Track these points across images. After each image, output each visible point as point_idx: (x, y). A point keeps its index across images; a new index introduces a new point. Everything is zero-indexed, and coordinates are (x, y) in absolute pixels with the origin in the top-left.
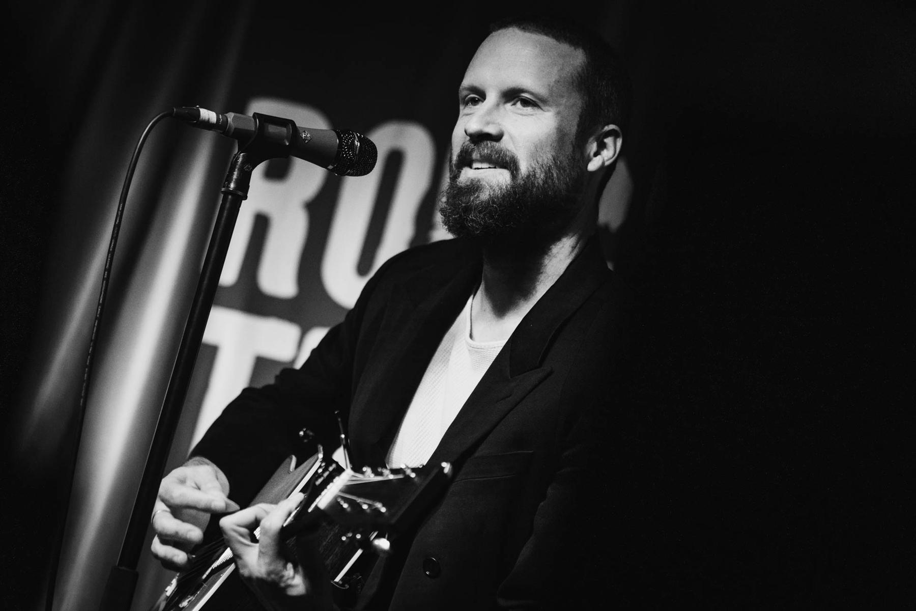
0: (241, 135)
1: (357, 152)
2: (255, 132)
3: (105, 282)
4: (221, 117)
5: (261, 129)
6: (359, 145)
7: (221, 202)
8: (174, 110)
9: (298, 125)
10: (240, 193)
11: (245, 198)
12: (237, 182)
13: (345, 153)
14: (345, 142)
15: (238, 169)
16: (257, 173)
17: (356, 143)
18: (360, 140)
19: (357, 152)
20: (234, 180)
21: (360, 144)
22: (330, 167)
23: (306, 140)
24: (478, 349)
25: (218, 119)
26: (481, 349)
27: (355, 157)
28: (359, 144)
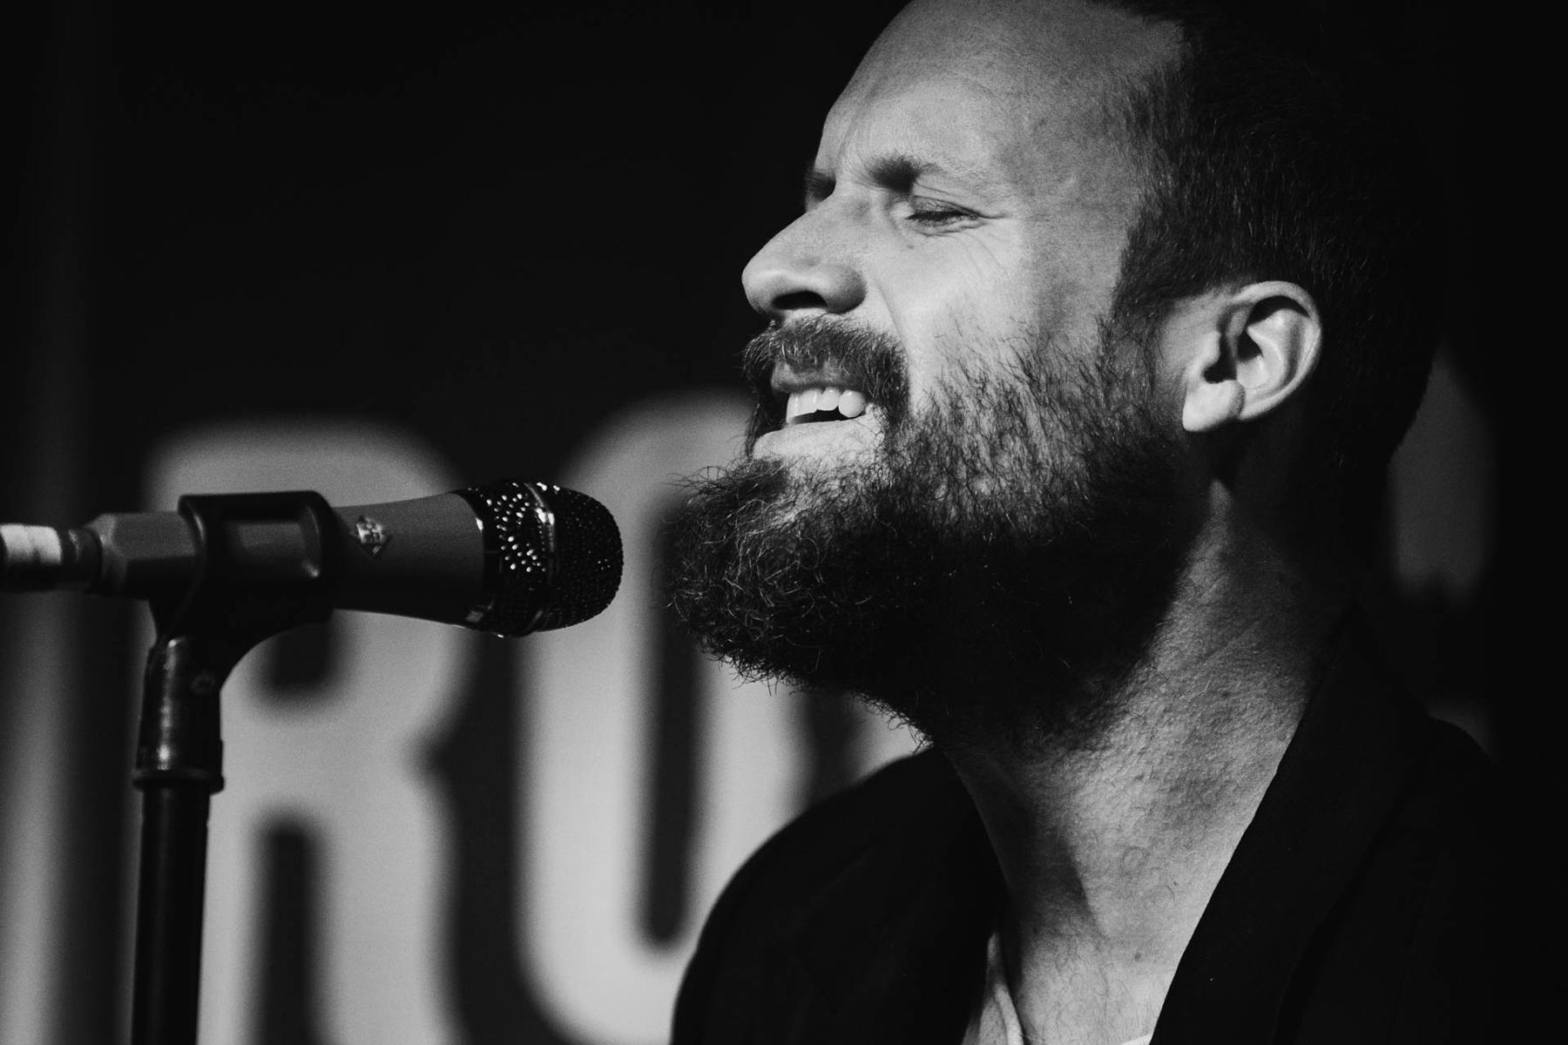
1: (552, 544)
5: (218, 543)
6: (552, 521)
7: (139, 818)
9: (335, 502)
11: (218, 784)
12: (177, 742)
13: (517, 561)
17: (542, 516)
18: (551, 502)
19: (552, 544)
20: (166, 735)
21: (555, 517)
22: (474, 616)
23: (373, 545)
28: (551, 517)
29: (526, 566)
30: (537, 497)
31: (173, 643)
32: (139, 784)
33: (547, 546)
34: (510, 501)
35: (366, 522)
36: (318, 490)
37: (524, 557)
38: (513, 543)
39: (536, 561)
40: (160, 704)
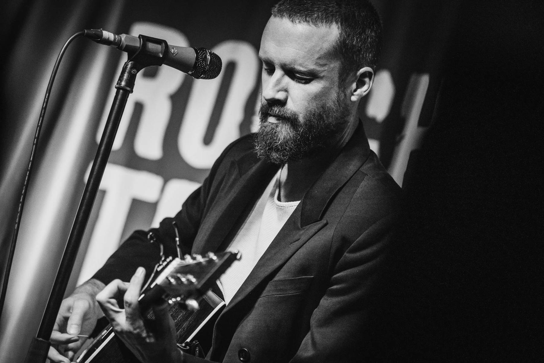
0: (130, 50)
1: (208, 63)
2: (140, 47)
3: (34, 146)
4: (117, 37)
5: (144, 45)
6: (210, 58)
8: (85, 31)
9: (168, 44)
10: (128, 89)
11: (132, 92)
14: (200, 56)
15: (128, 73)
16: (139, 75)
19: (208, 63)
20: (124, 80)
21: (210, 58)
23: (174, 54)
25: (115, 39)
28: (210, 57)
29: (202, 66)
30: (208, 53)
31: (130, 62)
32: (116, 87)
36: (166, 40)
39: (205, 65)
40: (125, 73)
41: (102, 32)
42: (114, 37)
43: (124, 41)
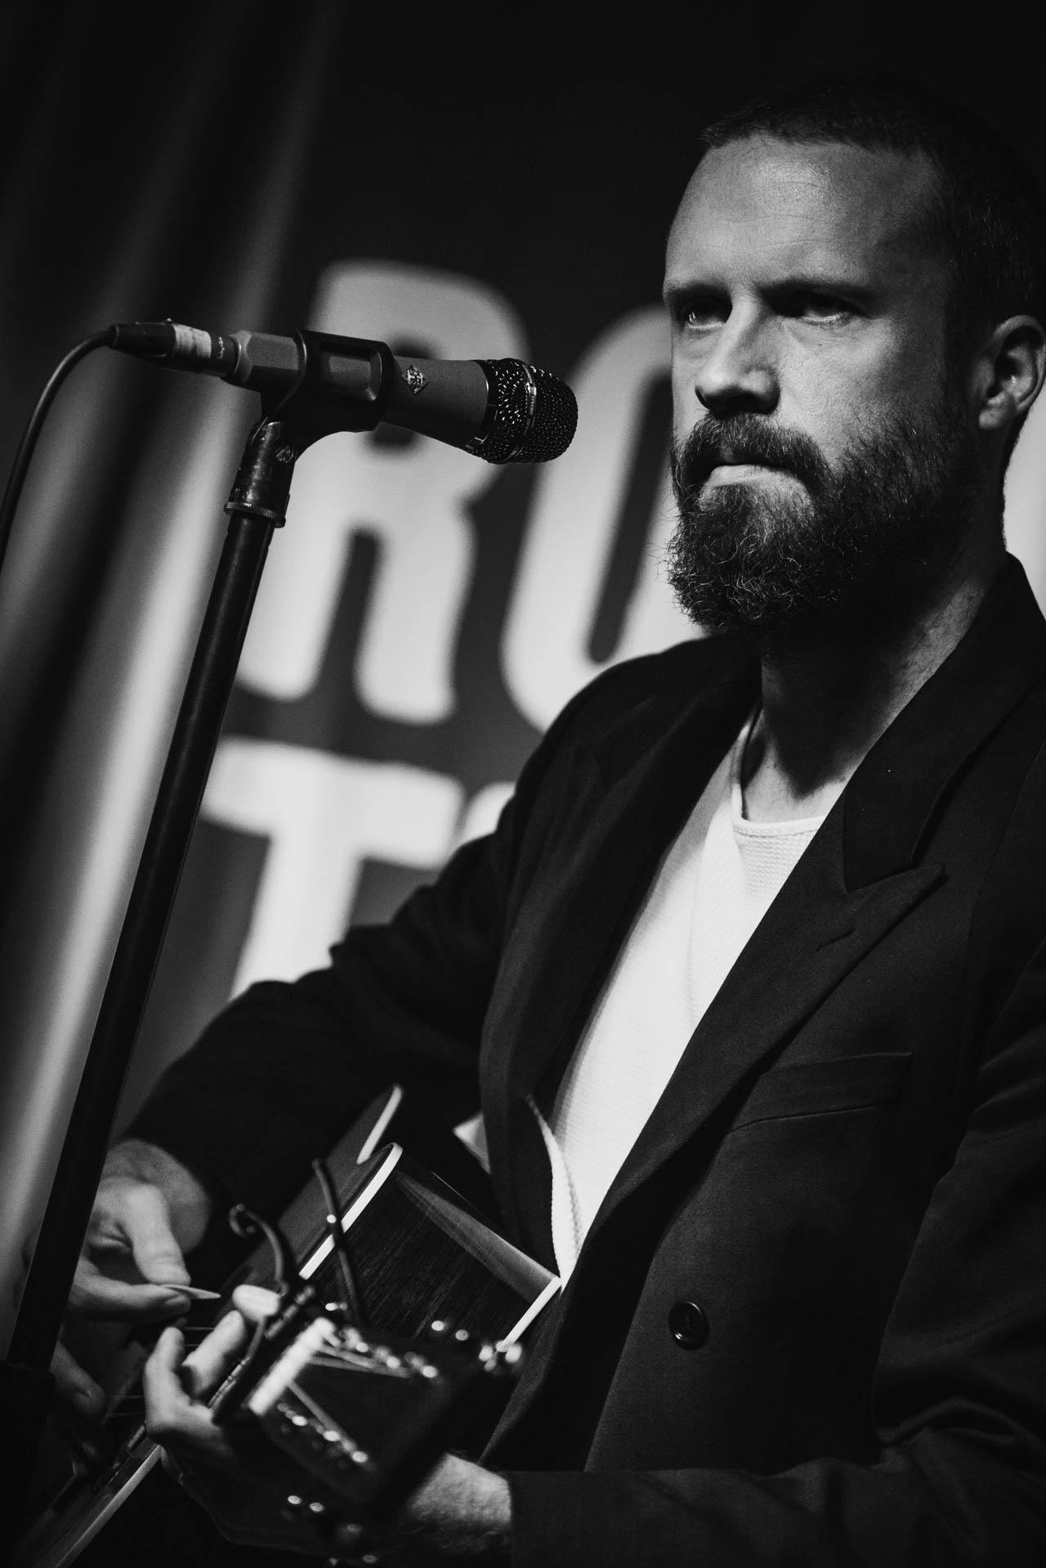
1: (532, 409)
2: (299, 372)
4: (221, 342)
6: (535, 393)
8: (115, 330)
10: (268, 513)
11: (282, 522)
15: (265, 460)
17: (529, 388)
19: (532, 409)
20: (254, 484)
23: (415, 387)
24: (764, 837)
25: (216, 348)
26: (771, 837)
27: (528, 423)
28: (535, 389)
29: (512, 420)
30: (529, 375)
31: (271, 424)
33: (529, 410)
34: (510, 375)
35: (413, 370)
37: (512, 414)
38: (507, 403)
39: (519, 418)
40: (256, 463)
41: (173, 332)
42: (212, 345)
43: (246, 355)
